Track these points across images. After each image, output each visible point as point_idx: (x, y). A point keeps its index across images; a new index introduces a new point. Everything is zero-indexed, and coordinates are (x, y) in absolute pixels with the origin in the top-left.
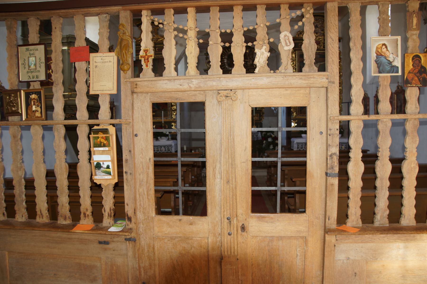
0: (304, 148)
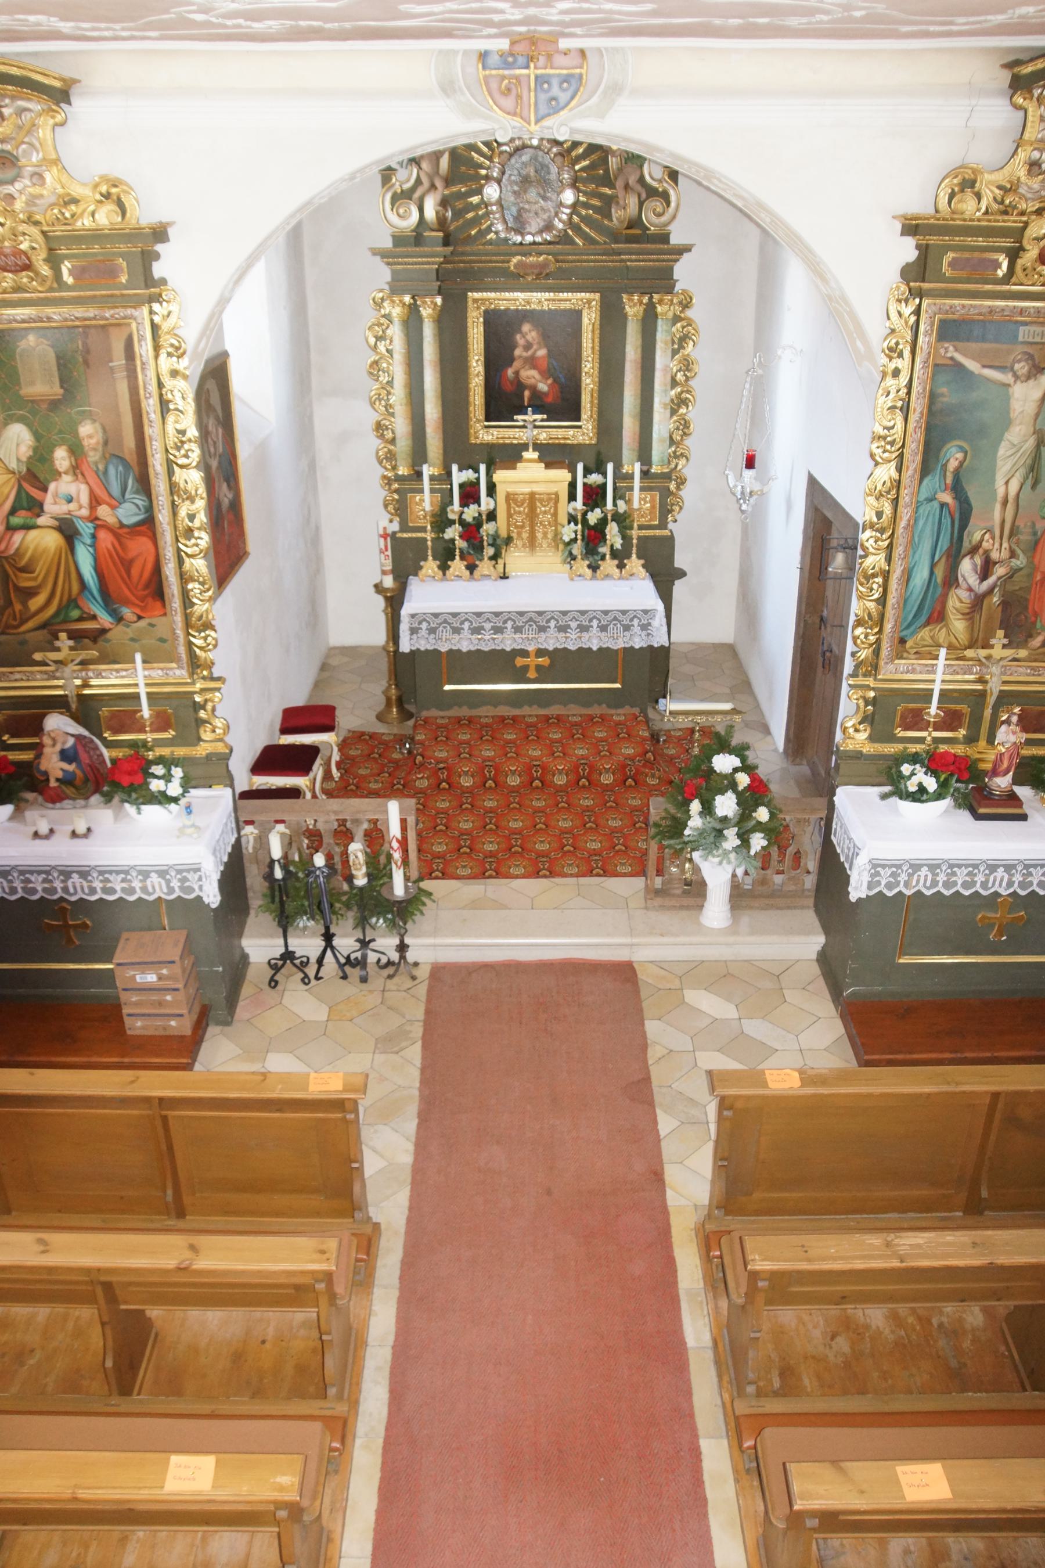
0: (902, 883)
